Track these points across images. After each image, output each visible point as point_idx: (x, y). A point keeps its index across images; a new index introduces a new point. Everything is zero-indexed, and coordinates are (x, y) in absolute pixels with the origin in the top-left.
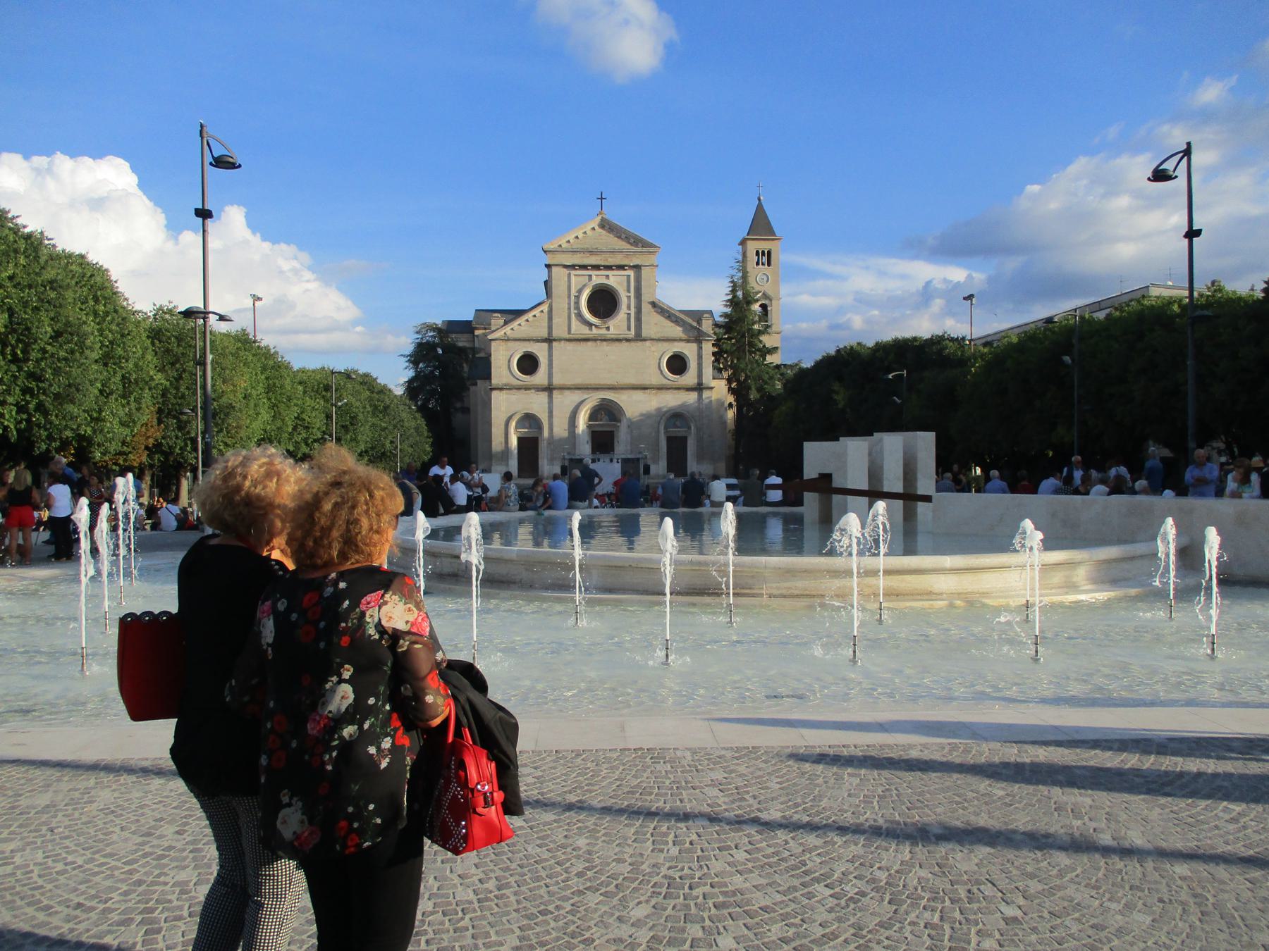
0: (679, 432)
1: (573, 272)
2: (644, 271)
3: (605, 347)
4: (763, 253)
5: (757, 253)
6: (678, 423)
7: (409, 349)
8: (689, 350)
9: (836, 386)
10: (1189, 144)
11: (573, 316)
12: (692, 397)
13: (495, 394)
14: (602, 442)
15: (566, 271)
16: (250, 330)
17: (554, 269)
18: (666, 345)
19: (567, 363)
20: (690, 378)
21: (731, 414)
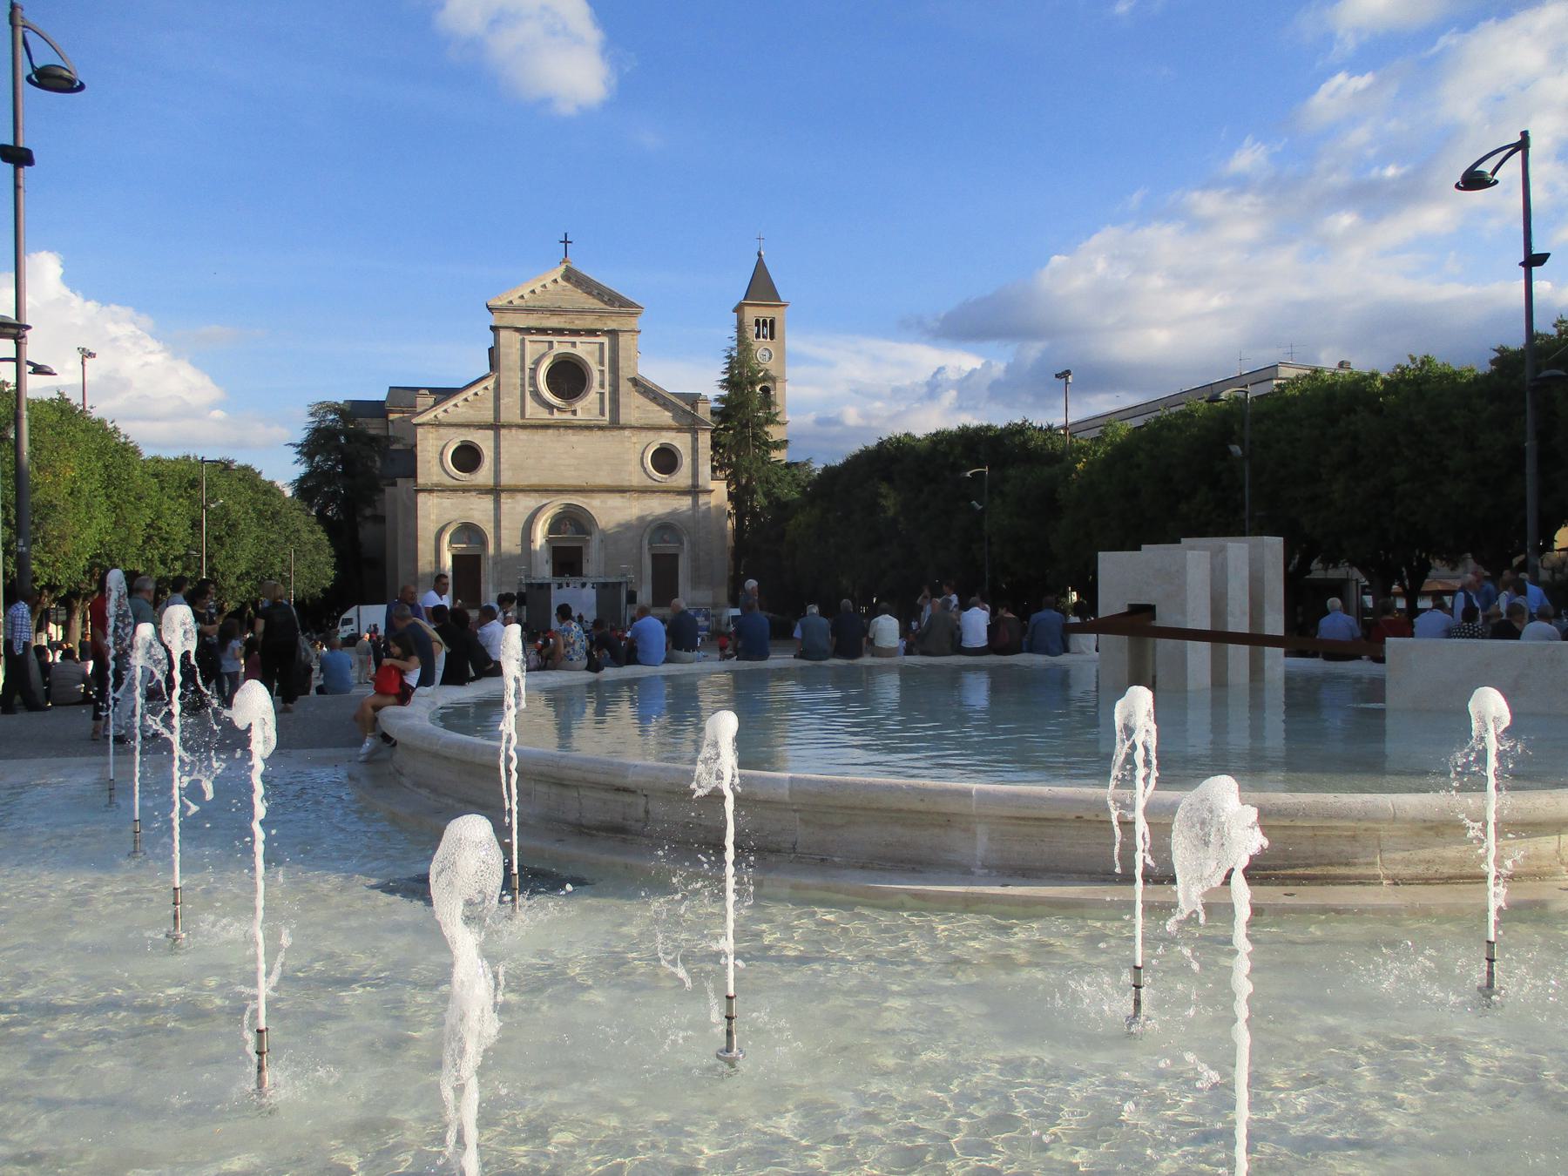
0: (668, 548)
1: (528, 338)
2: (623, 339)
3: (572, 437)
5: (757, 323)
7: (301, 436)
8: (681, 442)
9: (884, 488)
10: (1525, 134)
12: (685, 503)
13: (421, 497)
14: (567, 560)
15: (518, 336)
16: (76, 400)
17: (503, 333)
18: (651, 435)
19: (519, 456)
20: (682, 478)
21: (730, 524)
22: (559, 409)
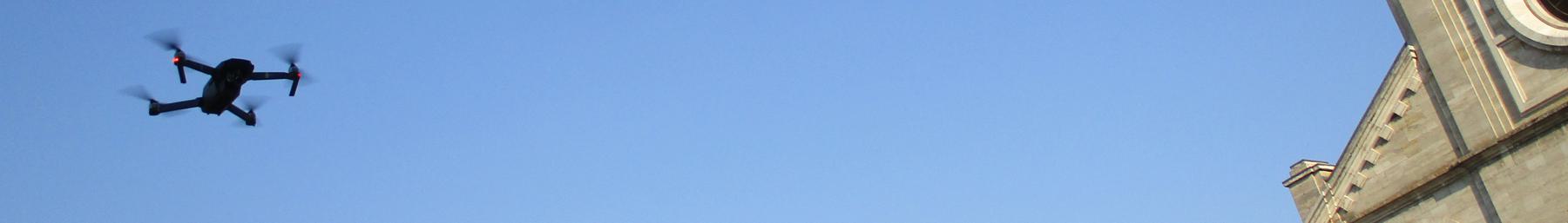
11: (1501, 57)
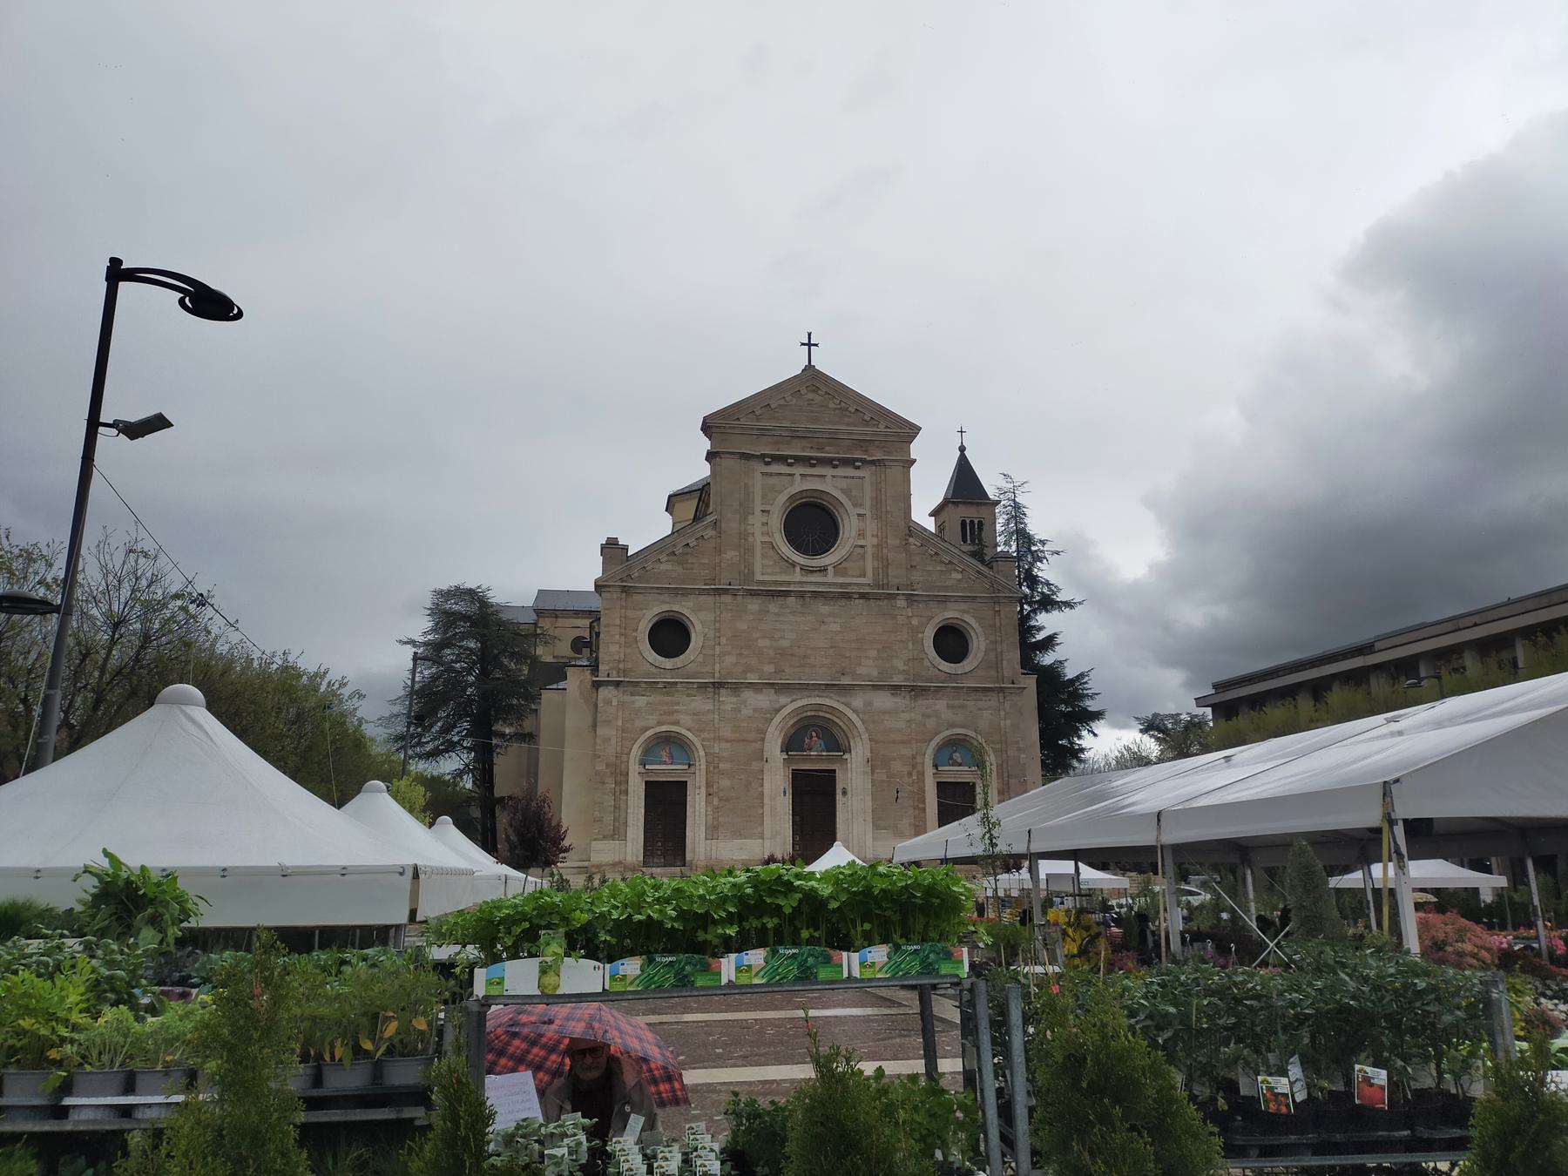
4: (972, 522)
5: (963, 523)
6: (957, 756)
22: (806, 570)
